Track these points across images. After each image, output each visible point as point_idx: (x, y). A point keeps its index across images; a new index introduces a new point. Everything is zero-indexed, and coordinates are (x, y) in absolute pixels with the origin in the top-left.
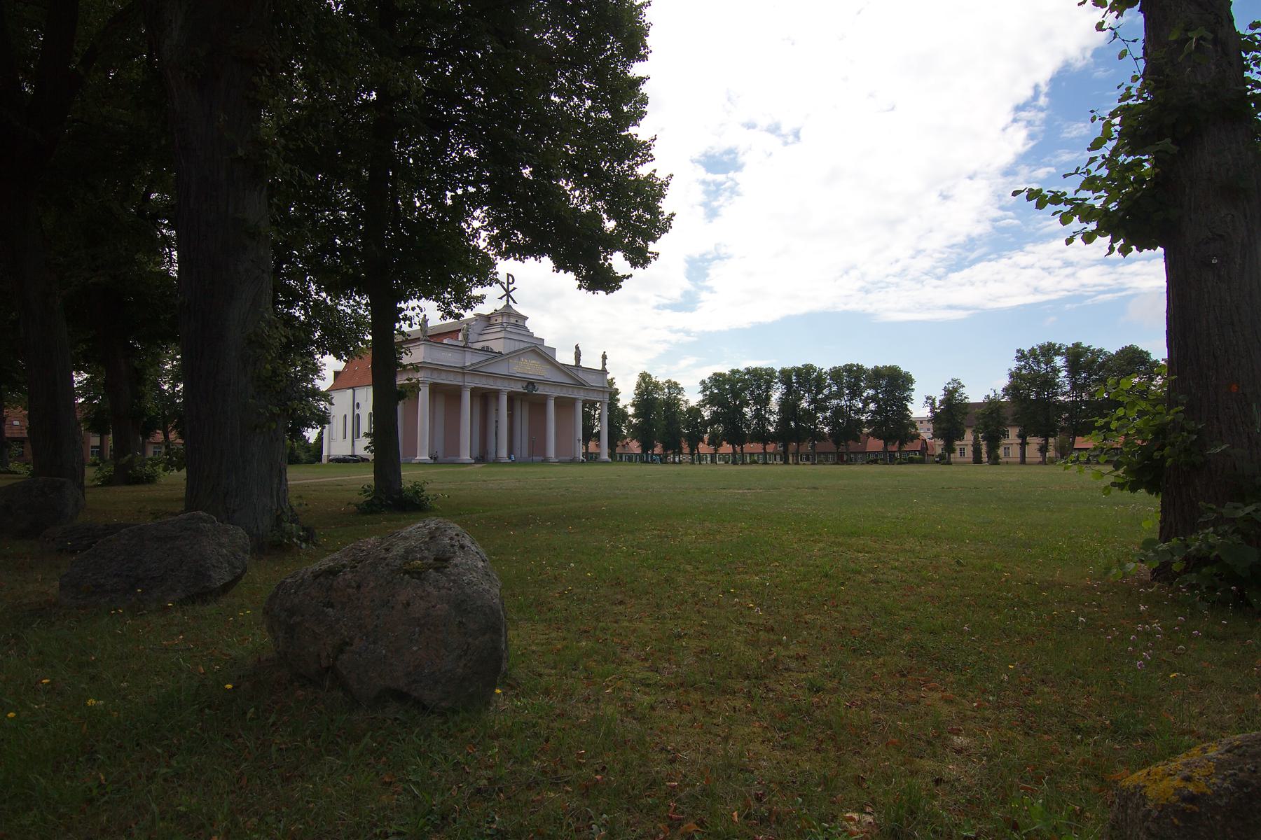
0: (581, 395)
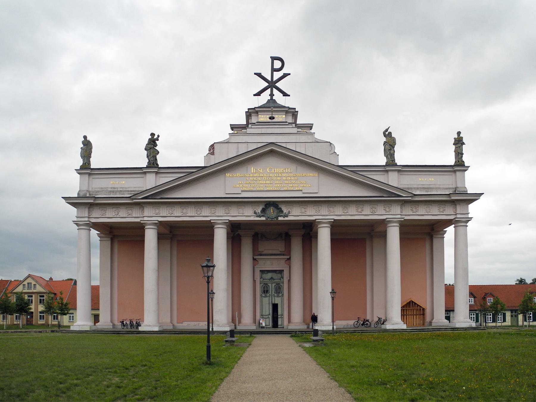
0: (396, 213)
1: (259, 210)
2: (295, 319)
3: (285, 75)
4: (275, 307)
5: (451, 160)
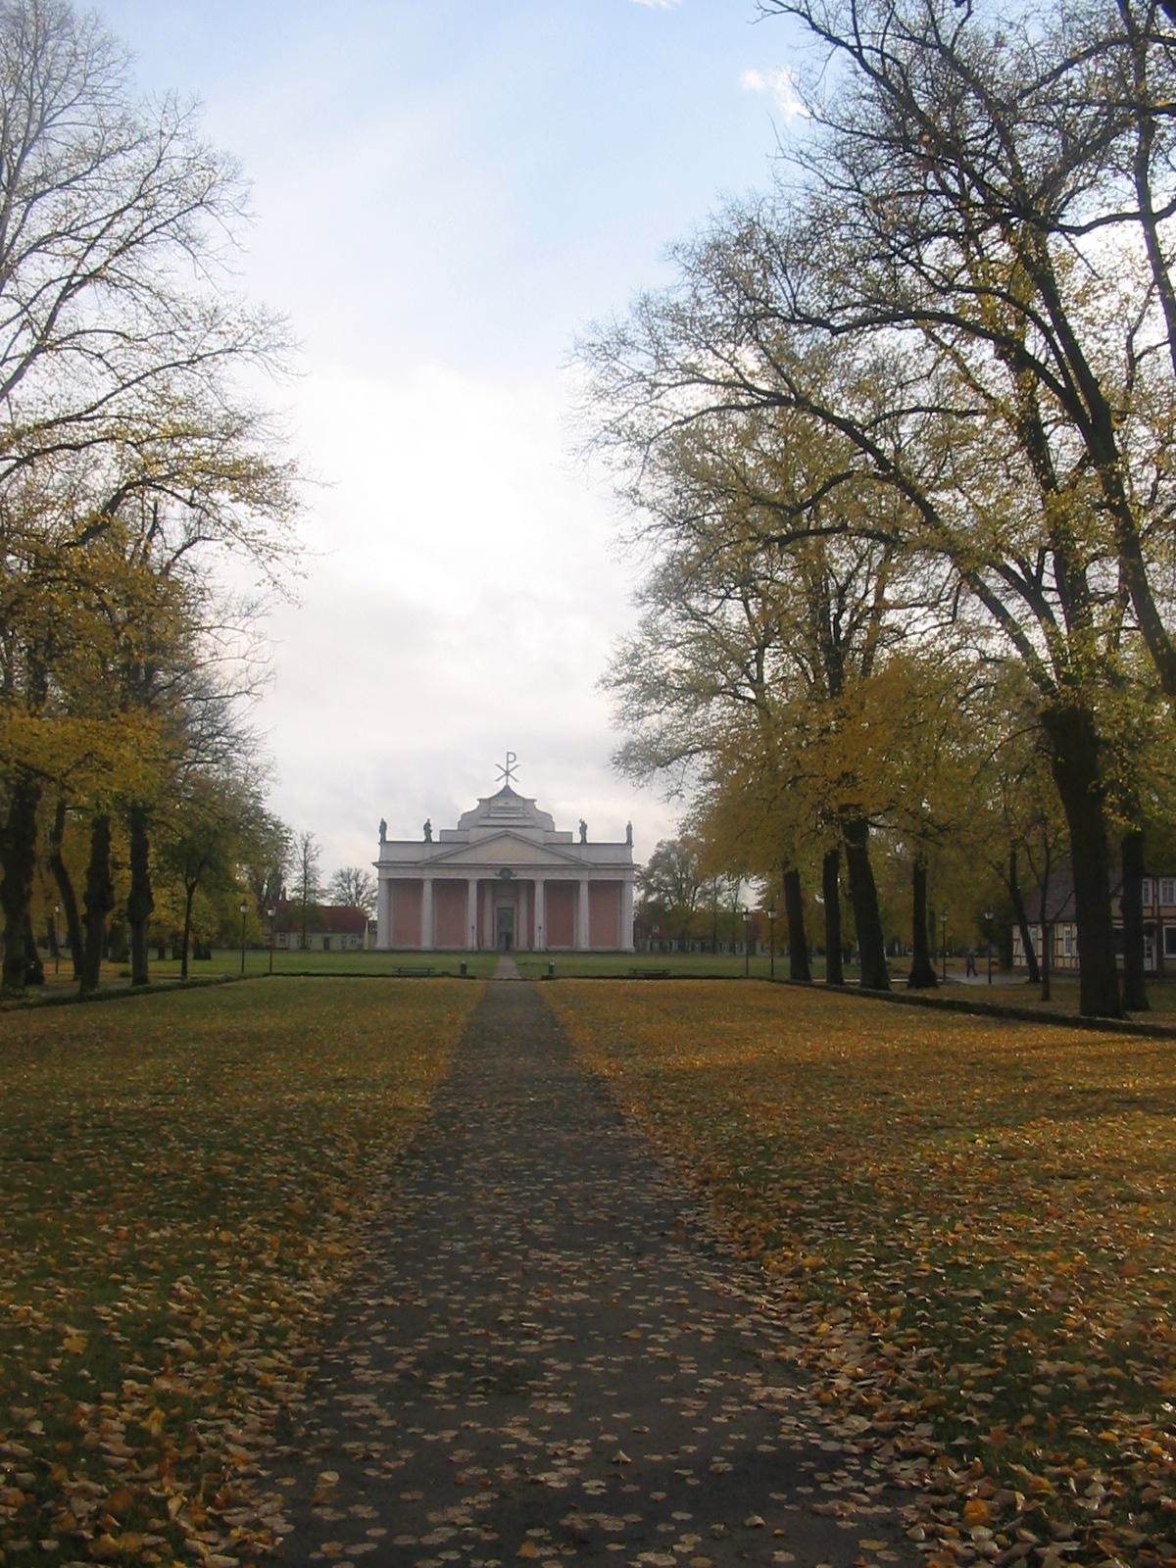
2: (521, 941)
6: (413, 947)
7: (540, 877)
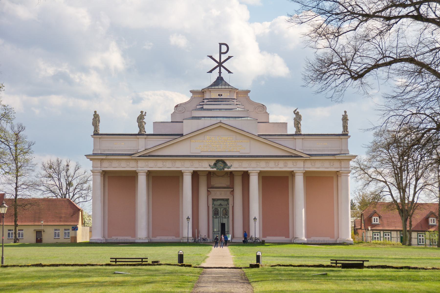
1: (212, 163)
3: (230, 57)
4: (223, 225)
5: (340, 131)
6: (129, 239)
7: (254, 168)
